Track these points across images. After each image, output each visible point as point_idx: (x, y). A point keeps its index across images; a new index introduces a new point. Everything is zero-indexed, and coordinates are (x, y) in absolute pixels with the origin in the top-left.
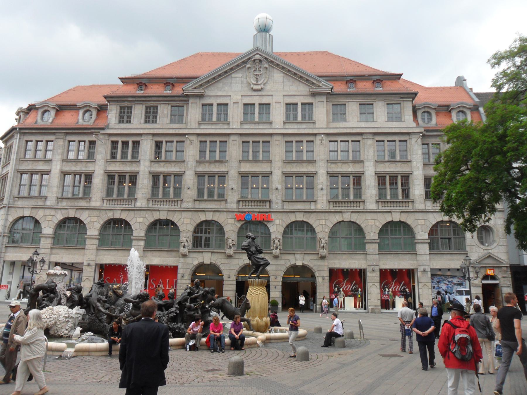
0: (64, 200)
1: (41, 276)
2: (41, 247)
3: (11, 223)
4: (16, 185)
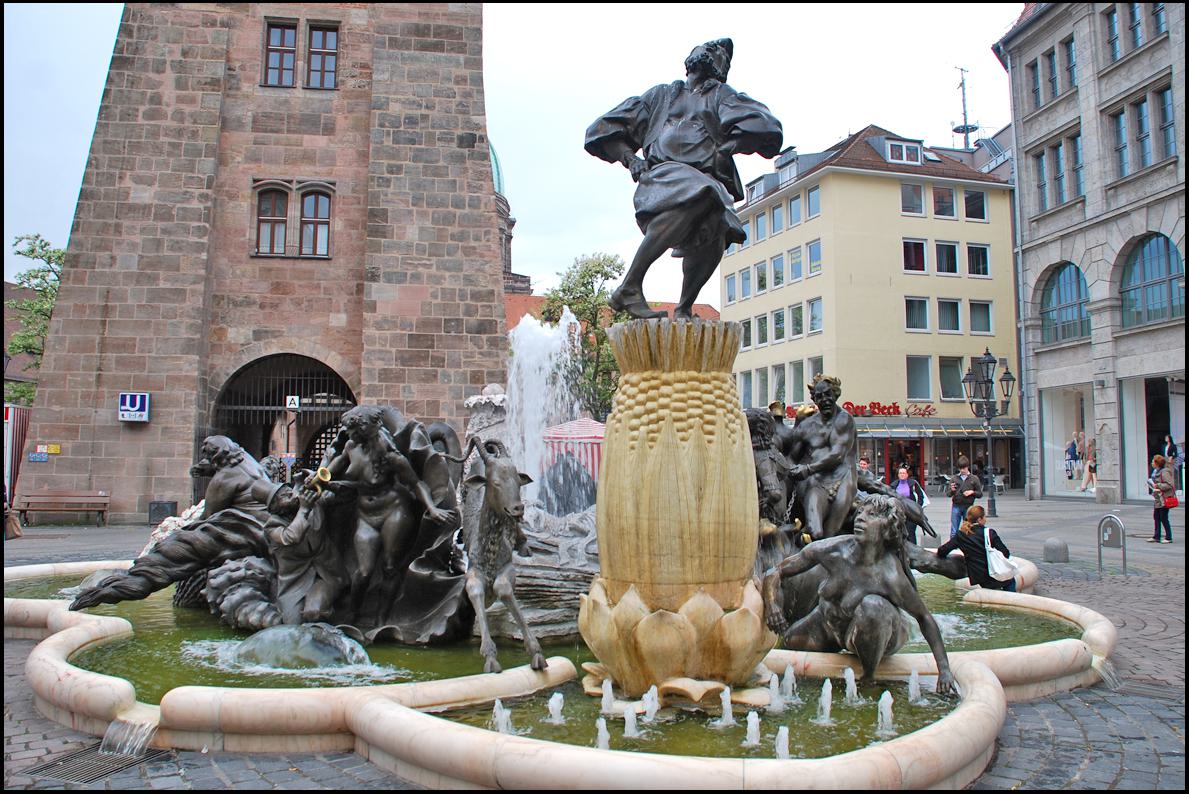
0: (1120, 191)
1: (1105, 422)
2: (1093, 340)
3: (1035, 290)
4: (1029, 190)
